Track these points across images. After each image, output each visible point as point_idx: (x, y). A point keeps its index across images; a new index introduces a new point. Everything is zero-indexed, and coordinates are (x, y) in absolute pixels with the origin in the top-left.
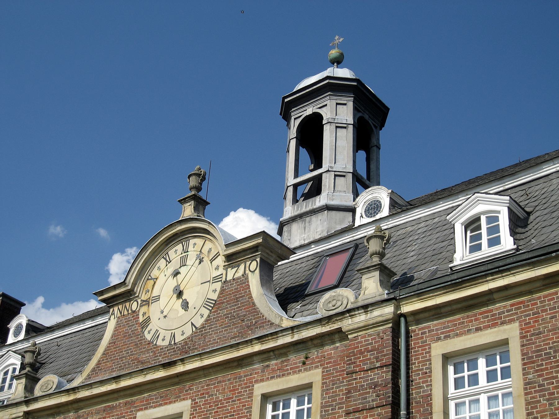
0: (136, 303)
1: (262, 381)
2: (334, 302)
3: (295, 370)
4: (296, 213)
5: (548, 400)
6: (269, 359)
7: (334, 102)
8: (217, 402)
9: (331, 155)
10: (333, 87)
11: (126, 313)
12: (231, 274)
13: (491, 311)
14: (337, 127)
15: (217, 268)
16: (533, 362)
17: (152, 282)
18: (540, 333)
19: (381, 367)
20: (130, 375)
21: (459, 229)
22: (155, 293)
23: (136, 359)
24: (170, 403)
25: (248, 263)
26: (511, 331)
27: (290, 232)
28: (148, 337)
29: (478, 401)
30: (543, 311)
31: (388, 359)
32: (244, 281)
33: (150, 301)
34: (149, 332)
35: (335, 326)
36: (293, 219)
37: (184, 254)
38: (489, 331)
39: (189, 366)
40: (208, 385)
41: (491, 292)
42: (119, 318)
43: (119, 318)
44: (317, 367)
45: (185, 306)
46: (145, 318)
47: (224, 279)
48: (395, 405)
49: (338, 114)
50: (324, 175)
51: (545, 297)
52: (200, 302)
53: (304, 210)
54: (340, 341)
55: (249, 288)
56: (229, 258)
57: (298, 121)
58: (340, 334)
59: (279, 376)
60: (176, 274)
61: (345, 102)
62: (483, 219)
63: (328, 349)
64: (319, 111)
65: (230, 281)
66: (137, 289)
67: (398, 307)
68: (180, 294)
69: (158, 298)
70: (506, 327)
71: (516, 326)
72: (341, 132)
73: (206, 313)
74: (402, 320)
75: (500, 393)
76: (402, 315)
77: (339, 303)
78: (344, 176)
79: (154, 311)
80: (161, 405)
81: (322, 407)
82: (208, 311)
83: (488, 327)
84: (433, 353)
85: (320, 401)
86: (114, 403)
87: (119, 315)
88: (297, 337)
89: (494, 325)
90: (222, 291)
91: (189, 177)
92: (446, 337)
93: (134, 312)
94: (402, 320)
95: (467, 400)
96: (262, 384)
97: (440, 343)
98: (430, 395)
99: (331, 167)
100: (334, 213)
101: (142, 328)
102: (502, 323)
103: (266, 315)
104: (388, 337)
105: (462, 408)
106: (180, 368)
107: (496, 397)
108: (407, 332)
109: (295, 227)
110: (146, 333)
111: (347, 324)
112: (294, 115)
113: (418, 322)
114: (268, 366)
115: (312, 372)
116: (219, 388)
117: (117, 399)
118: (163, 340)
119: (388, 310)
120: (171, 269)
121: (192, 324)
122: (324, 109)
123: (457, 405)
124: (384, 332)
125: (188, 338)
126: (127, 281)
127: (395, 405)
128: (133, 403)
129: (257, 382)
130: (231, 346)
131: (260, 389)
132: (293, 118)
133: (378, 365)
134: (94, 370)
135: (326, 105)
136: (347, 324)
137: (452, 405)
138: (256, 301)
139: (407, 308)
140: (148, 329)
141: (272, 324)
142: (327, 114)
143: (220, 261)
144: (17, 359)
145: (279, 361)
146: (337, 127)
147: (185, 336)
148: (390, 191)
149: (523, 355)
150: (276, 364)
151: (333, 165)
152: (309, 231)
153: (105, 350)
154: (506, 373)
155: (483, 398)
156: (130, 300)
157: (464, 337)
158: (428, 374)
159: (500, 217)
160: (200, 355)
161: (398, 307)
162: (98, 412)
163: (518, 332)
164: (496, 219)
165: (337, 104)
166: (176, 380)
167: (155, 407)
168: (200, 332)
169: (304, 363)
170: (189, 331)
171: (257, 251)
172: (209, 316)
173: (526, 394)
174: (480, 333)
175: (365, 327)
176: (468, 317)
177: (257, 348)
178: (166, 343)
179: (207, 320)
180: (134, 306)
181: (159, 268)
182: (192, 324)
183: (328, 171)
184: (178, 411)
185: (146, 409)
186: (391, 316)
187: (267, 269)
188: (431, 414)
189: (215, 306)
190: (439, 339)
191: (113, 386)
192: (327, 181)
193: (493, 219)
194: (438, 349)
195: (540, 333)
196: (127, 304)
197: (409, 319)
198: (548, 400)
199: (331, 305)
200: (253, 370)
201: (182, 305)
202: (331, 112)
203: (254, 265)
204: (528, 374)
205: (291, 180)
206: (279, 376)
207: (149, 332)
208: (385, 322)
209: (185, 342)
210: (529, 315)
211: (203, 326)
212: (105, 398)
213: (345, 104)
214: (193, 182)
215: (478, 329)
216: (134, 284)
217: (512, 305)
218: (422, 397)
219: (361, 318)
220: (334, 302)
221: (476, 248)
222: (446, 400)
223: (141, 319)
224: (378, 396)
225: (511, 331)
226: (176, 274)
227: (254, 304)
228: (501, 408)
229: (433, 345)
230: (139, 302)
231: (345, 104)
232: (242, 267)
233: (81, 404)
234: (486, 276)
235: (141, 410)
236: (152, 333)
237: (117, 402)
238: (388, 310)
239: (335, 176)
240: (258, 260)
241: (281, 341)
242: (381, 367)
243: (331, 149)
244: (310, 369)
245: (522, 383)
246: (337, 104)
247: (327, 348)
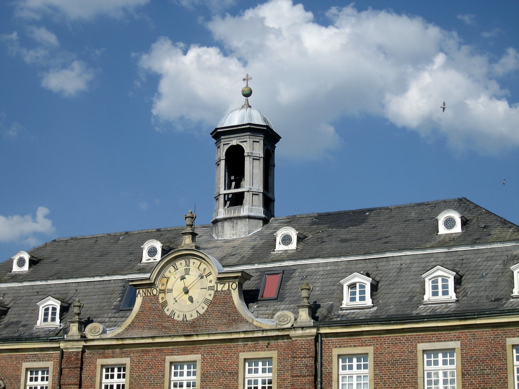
0: (155, 290)
1: (244, 351)
2: (283, 318)
3: (262, 349)
4: (228, 216)
5: (384, 383)
6: (248, 341)
7: (252, 140)
8: (218, 358)
9: (250, 180)
10: (251, 130)
11: (149, 295)
12: (220, 287)
13: (361, 339)
14: (253, 159)
15: (211, 281)
16: (378, 366)
17: (165, 280)
18: (382, 353)
19: (309, 357)
20: (162, 337)
21: (345, 288)
22: (169, 286)
23: (160, 325)
24: (188, 354)
25: (231, 284)
26: (370, 350)
27: (223, 227)
28: (168, 313)
29: (352, 377)
30: (385, 344)
31: (313, 354)
32: (228, 293)
33: (166, 292)
34: (168, 310)
35: (286, 333)
36: (225, 219)
37: (186, 267)
38: (360, 348)
39: (201, 338)
40: (211, 348)
41: (362, 331)
42: (144, 297)
43: (144, 297)
44: (274, 350)
45: (191, 299)
46: (163, 301)
47: (215, 289)
48: (316, 376)
49: (253, 148)
50: (246, 193)
51: (386, 337)
52: (201, 300)
53: (232, 215)
54: (287, 339)
55: (232, 298)
56: (219, 279)
57: (227, 147)
58: (288, 337)
59: (254, 351)
60: (183, 278)
61: (258, 140)
62: (358, 285)
63: (280, 342)
64: (241, 144)
65: (220, 291)
66: (157, 283)
67: (318, 330)
68: (186, 292)
69: (171, 291)
70: (367, 347)
71: (372, 348)
72: (256, 163)
73: (206, 307)
74: (319, 335)
75: (362, 375)
76: (319, 333)
77: (286, 319)
78: (258, 195)
79: (169, 298)
80: (181, 354)
81: (278, 370)
82: (207, 307)
83: (359, 346)
84: (333, 353)
85: (277, 367)
86: (149, 349)
87: (144, 295)
88: (265, 334)
89: (362, 346)
90: (215, 296)
91: (186, 218)
92: (340, 347)
93: (155, 295)
94: (319, 335)
95: (347, 376)
96: (243, 353)
97: (336, 349)
98: (331, 372)
99: (250, 189)
100: (252, 220)
101: (163, 307)
102: (366, 345)
103: (244, 316)
104: (313, 343)
105: (345, 379)
106: (195, 338)
107: (361, 376)
108: (321, 340)
109: (227, 225)
110: (165, 310)
111: (292, 333)
112: (223, 141)
113: (326, 337)
114: (247, 344)
115: (272, 352)
116: (219, 351)
117: (151, 347)
118: (178, 317)
119: (314, 331)
120: (179, 275)
121: (197, 311)
122: (245, 143)
123: (342, 377)
124: (311, 340)
125: (195, 319)
126: (151, 278)
127: (316, 376)
128: (162, 350)
129: (240, 351)
130: (227, 333)
131: (243, 356)
132: (222, 143)
133: (308, 356)
134: (129, 326)
135: (246, 141)
136: (292, 333)
137: (340, 377)
138: (237, 307)
139: (323, 331)
140: (167, 308)
141: (247, 321)
142: (247, 148)
143: (214, 281)
144: (58, 303)
145: (253, 343)
146: (253, 159)
147: (192, 318)
148: (298, 232)
149: (374, 362)
150: (251, 344)
151: (251, 187)
152: (236, 230)
153: (137, 315)
154: (365, 367)
155: (355, 377)
156: (151, 288)
157: (348, 349)
158: (330, 362)
159: (366, 286)
160: (208, 334)
161: (318, 330)
162: (137, 352)
163: (373, 351)
164: (364, 287)
165: (254, 141)
166: (192, 343)
167: (178, 355)
168: (202, 317)
169: (267, 347)
170: (195, 316)
171: (237, 279)
172: (208, 309)
173: (375, 379)
174: (355, 348)
175: (302, 336)
176: (350, 339)
177: (242, 336)
178: (180, 319)
179: (206, 311)
180: (155, 292)
181: (170, 272)
182: (197, 311)
183: (249, 191)
184: (194, 359)
185: (172, 355)
186: (315, 334)
187: (240, 285)
188: (332, 381)
189: (212, 304)
190: (336, 347)
191: (150, 341)
192: (247, 197)
193: (362, 286)
194: (336, 352)
195: (382, 353)
196: (149, 290)
197: (322, 335)
198: (384, 383)
199: (281, 319)
200: (238, 345)
201: (189, 299)
202: (250, 148)
203: (234, 286)
204: (376, 370)
205: (223, 191)
206: (253, 351)
207: (168, 310)
208: (312, 336)
209: (194, 321)
210: (378, 344)
211: (204, 314)
212: (143, 345)
213: (258, 142)
214: (188, 221)
215: (355, 346)
216: (155, 280)
217: (371, 338)
218: (328, 373)
219: (299, 332)
220: (283, 318)
221: (353, 299)
222: (338, 375)
223: (161, 301)
224: (308, 371)
225: (370, 350)
226: (183, 278)
227: (235, 307)
228: (362, 382)
229: (333, 349)
230: (158, 291)
231: (258, 142)
232: (227, 285)
233: (125, 346)
234: (361, 325)
235: (169, 355)
236: (170, 311)
237: (151, 348)
238: (314, 331)
239: (253, 194)
240: (237, 283)
241: (256, 335)
242: (309, 357)
243: (250, 175)
244: (271, 350)
245: (373, 374)
246: (254, 141)
247: (279, 341)
